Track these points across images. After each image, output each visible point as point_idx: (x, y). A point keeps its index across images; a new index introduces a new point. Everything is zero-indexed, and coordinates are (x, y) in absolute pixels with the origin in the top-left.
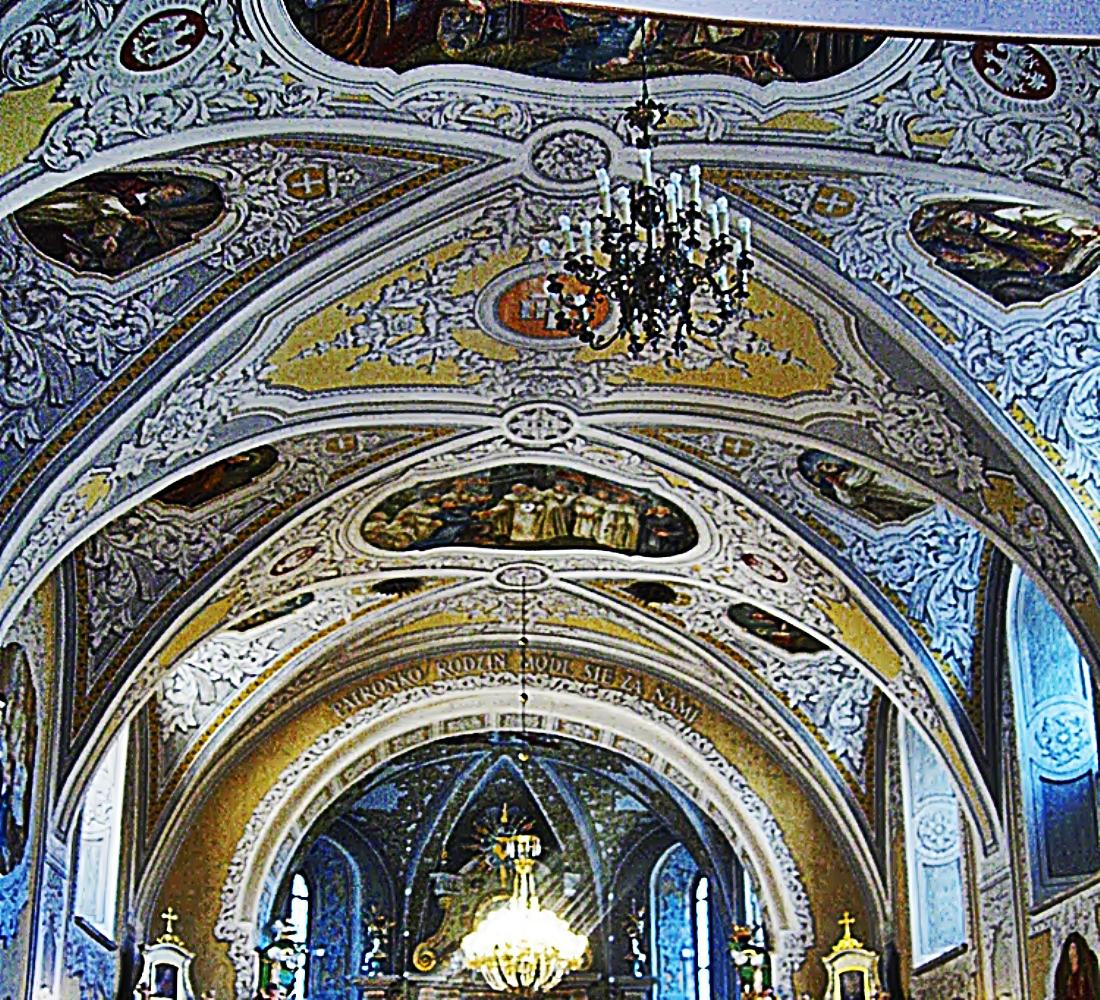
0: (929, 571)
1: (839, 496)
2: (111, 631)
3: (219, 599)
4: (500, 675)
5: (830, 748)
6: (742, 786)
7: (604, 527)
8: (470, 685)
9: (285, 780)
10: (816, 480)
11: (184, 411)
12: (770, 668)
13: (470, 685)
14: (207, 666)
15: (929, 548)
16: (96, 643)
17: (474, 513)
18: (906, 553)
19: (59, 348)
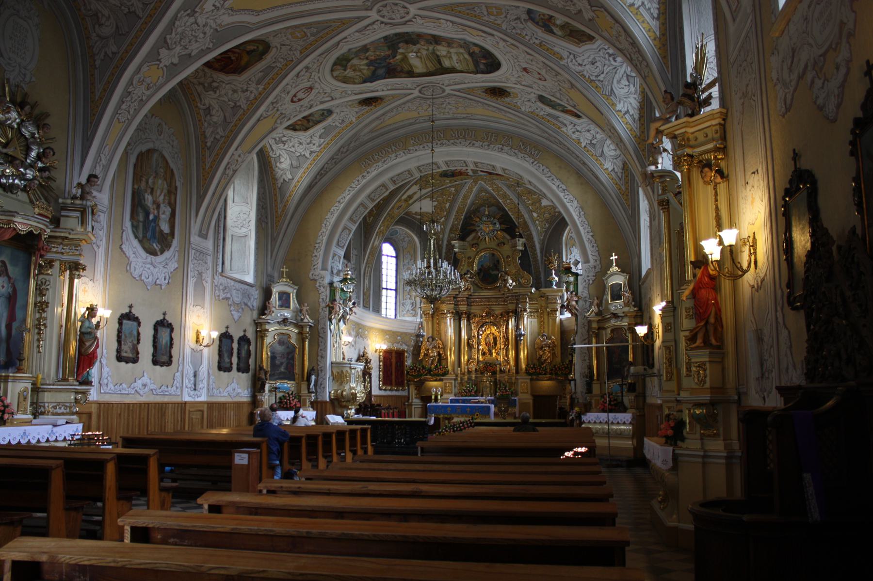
0: (611, 68)
1: (555, 31)
2: (215, 138)
3: (265, 118)
4: (441, 142)
5: (605, 167)
6: (564, 190)
7: (455, 61)
8: (426, 148)
9: (339, 202)
10: (541, 24)
11: (188, 29)
12: (570, 127)
13: (426, 148)
14: (293, 149)
15: (610, 55)
16: (209, 144)
17: (388, 61)
18: (597, 59)
19: (117, 6)
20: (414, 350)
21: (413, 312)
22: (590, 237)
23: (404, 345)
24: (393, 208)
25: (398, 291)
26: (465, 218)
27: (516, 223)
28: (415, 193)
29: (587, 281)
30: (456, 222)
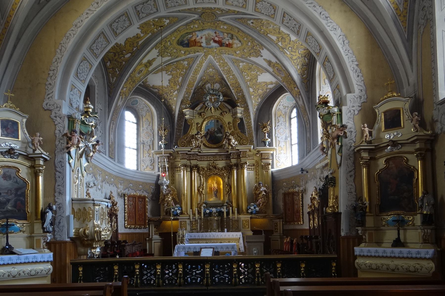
22: (355, 66)
26: (194, 93)
27: (236, 97)
29: (352, 111)
30: (187, 95)
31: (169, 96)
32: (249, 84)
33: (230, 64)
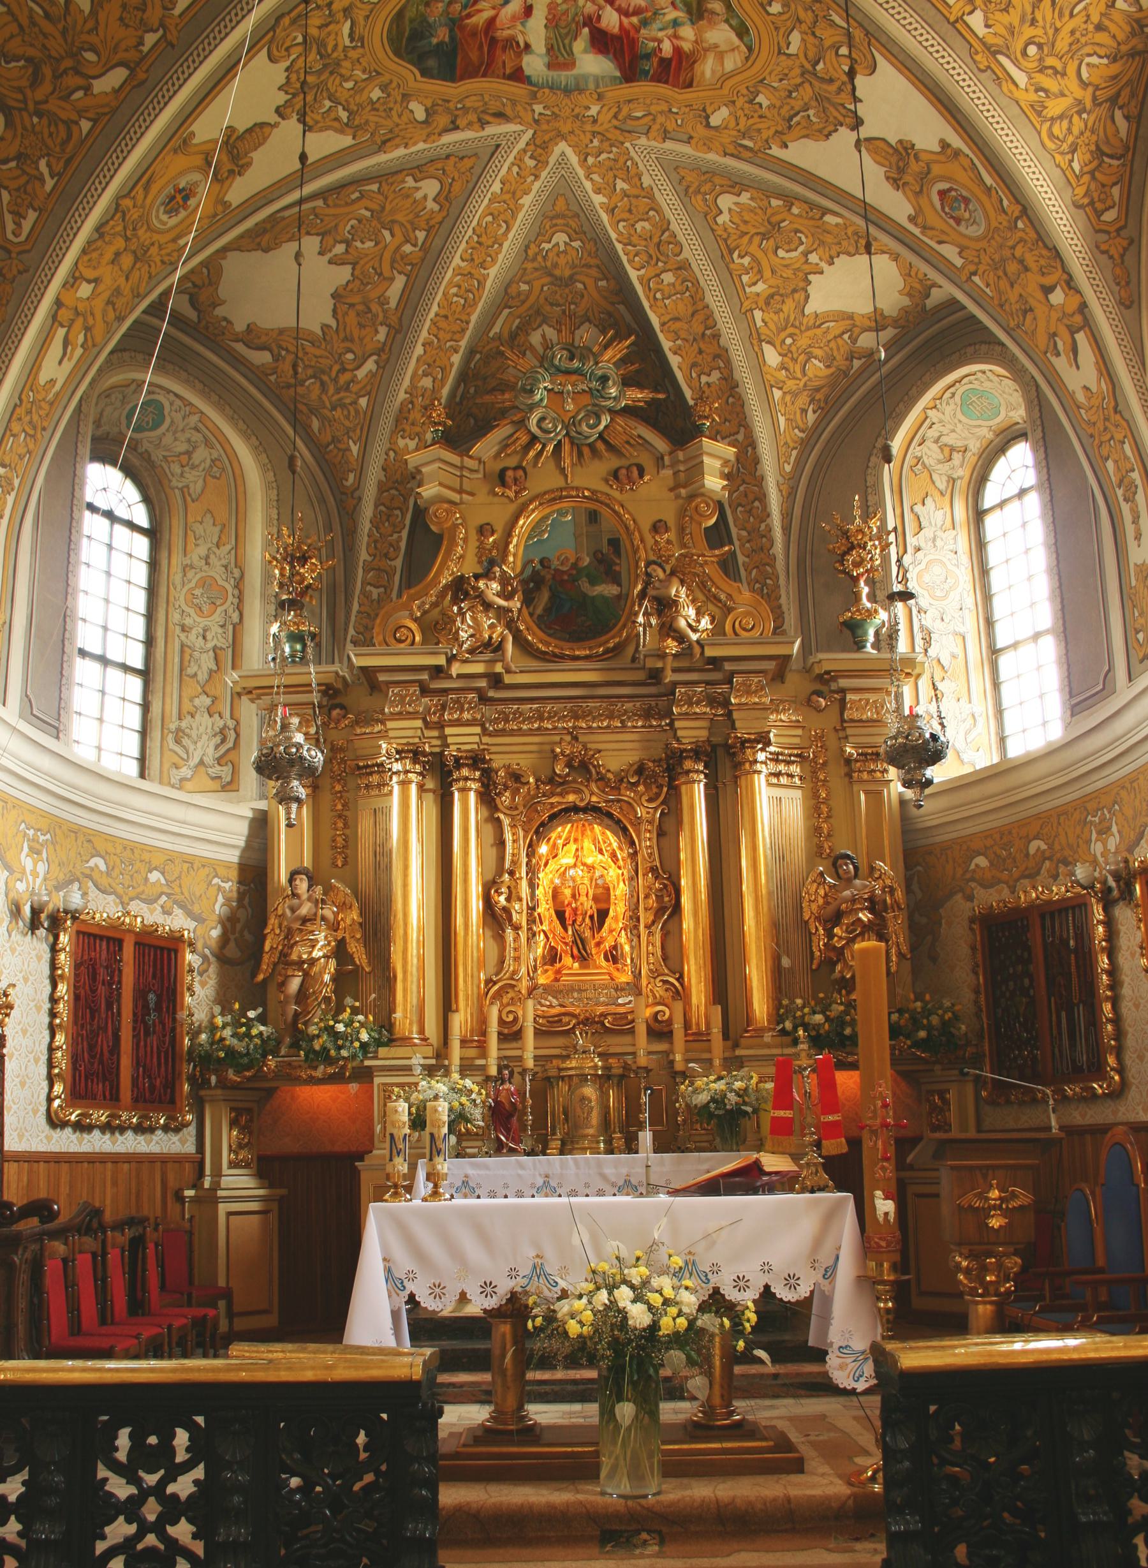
20: (224, 939)
21: (226, 772)
23: (177, 911)
24: (144, 177)
25: (159, 678)
26: (464, 377)
27: (688, 394)
28: (258, 132)
31: (331, 391)
32: (759, 324)
33: (667, 199)
